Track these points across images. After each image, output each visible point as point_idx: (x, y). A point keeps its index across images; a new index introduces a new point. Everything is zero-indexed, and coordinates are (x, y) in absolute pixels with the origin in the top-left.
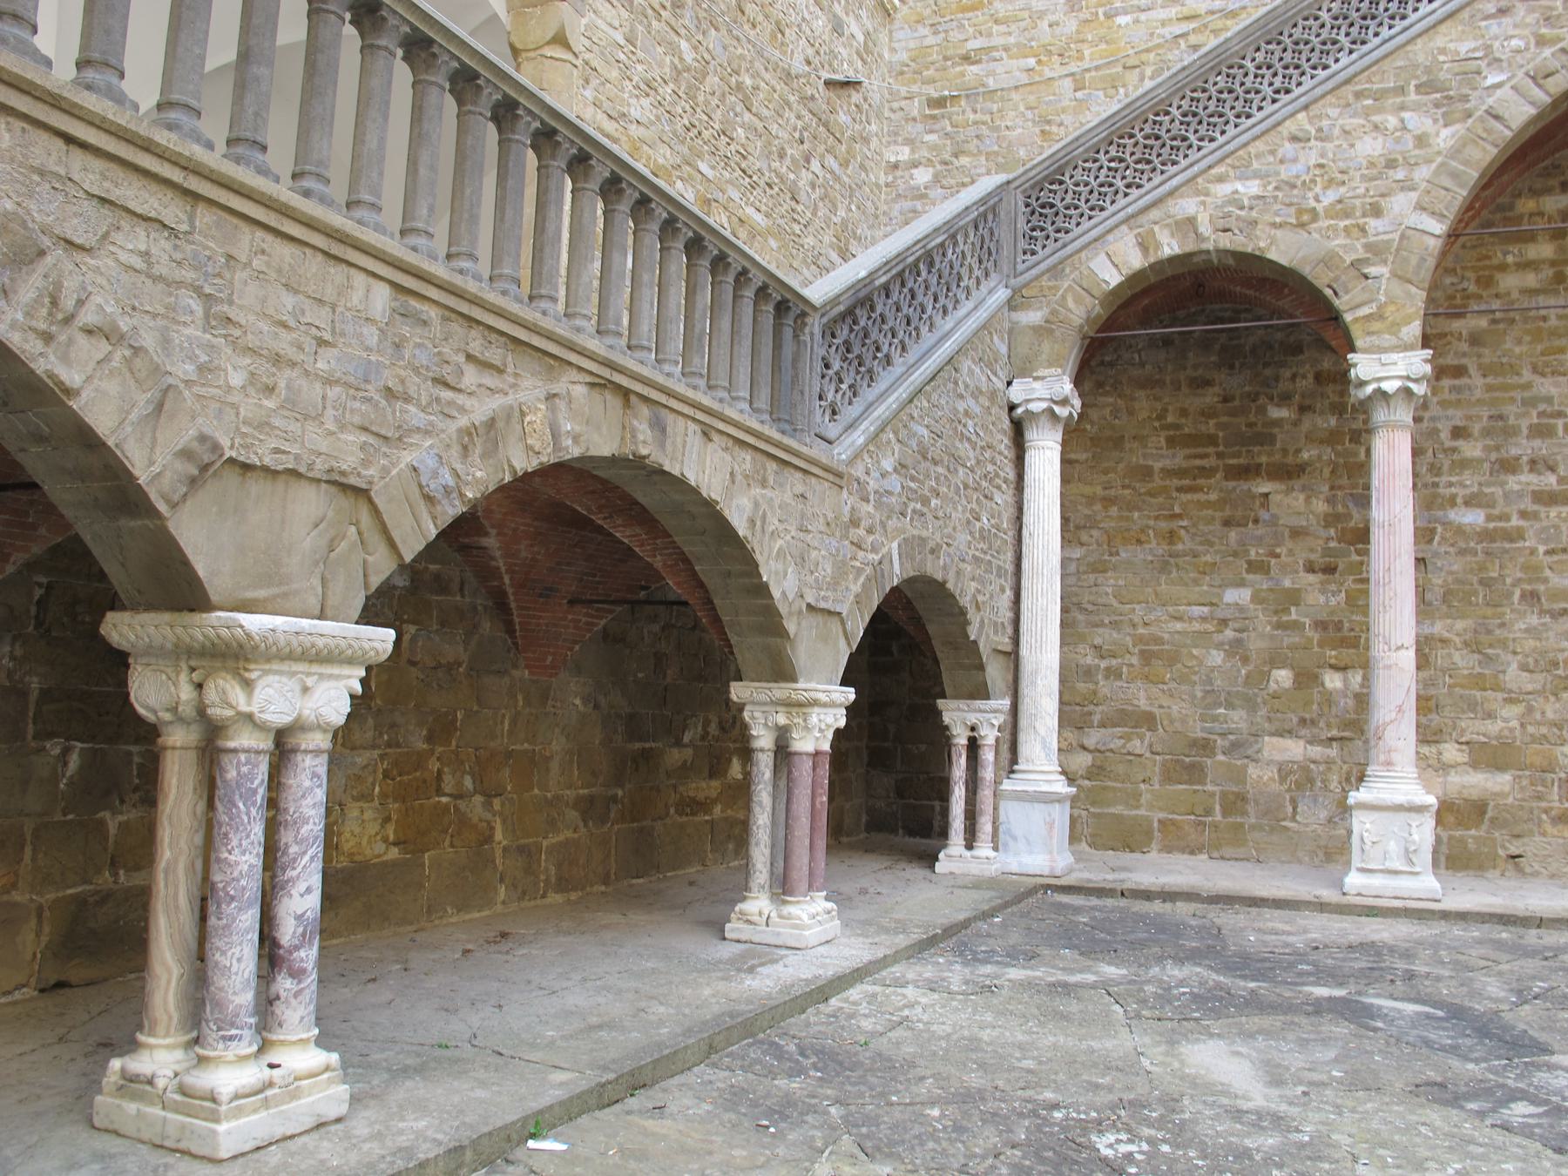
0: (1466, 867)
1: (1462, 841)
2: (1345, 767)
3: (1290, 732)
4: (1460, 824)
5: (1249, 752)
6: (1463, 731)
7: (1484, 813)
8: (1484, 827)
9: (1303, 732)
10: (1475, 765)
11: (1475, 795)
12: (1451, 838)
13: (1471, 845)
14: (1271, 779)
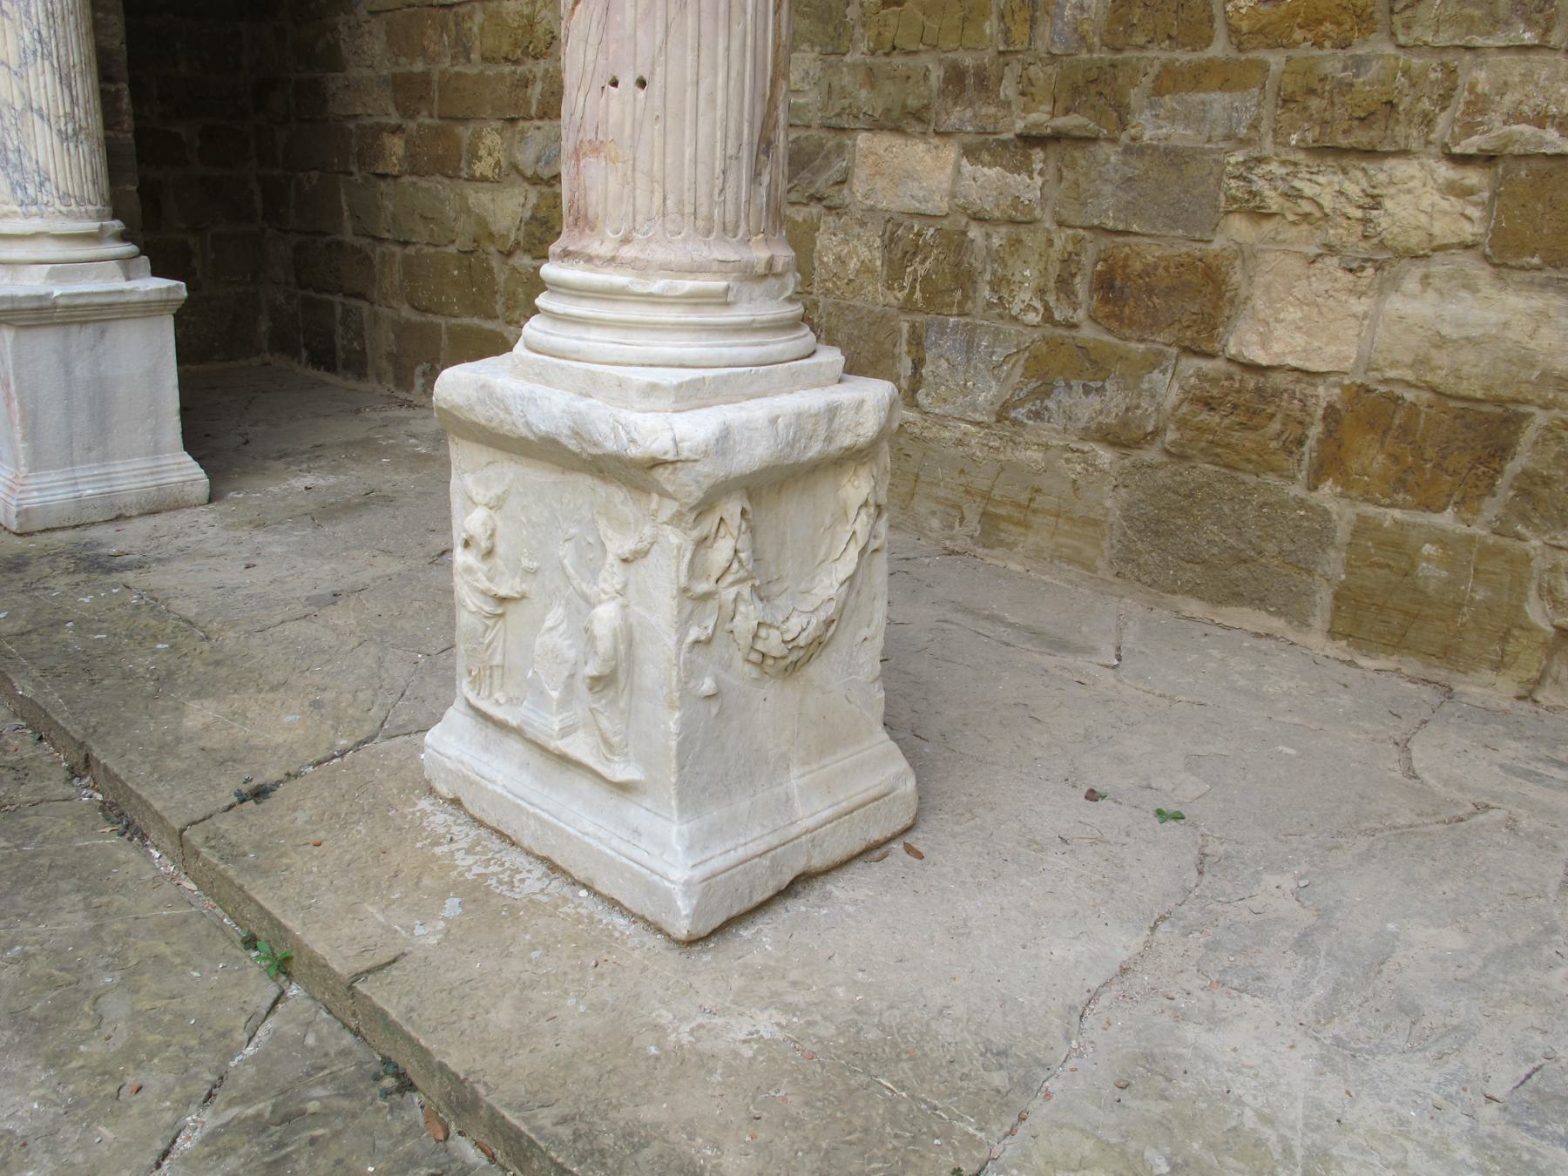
0: (1396, 643)
1: (1398, 545)
2: (1061, 239)
3: (919, 116)
4: (1412, 483)
5: (821, 184)
6: (1479, 104)
7: (1502, 451)
8: (1491, 508)
9: (958, 116)
10: (1503, 253)
11: (1473, 374)
12: (1363, 527)
13: (1431, 571)
14: (866, 268)
